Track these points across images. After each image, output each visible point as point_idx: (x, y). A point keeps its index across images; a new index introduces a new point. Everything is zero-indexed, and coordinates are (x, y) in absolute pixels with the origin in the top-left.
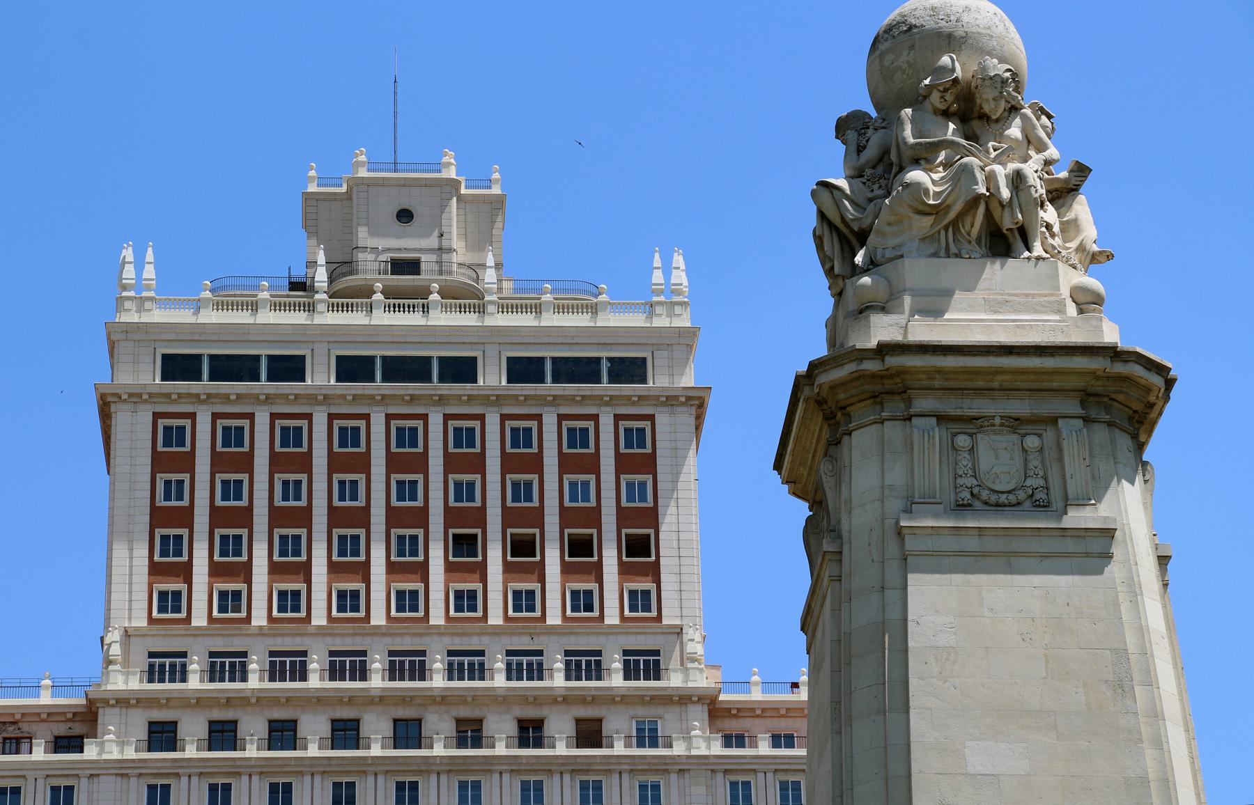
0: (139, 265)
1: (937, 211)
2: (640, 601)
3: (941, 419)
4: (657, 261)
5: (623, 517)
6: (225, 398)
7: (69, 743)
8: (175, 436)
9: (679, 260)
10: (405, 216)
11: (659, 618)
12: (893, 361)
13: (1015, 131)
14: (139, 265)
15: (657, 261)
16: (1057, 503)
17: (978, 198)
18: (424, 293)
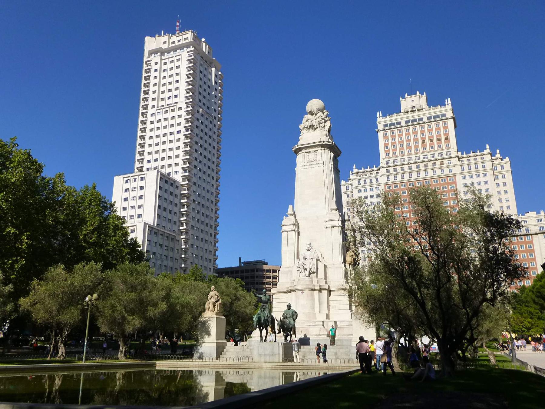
0: (380, 114)
1: (307, 128)
2: (448, 145)
3: (305, 153)
4: (446, 100)
5: (444, 134)
6: (391, 129)
7: (377, 173)
8: (386, 134)
9: (449, 100)
10: (413, 101)
11: (450, 147)
12: (299, 147)
13: (318, 115)
14: (380, 114)
15: (446, 100)
16: (318, 160)
17: (310, 125)
18: (415, 111)
